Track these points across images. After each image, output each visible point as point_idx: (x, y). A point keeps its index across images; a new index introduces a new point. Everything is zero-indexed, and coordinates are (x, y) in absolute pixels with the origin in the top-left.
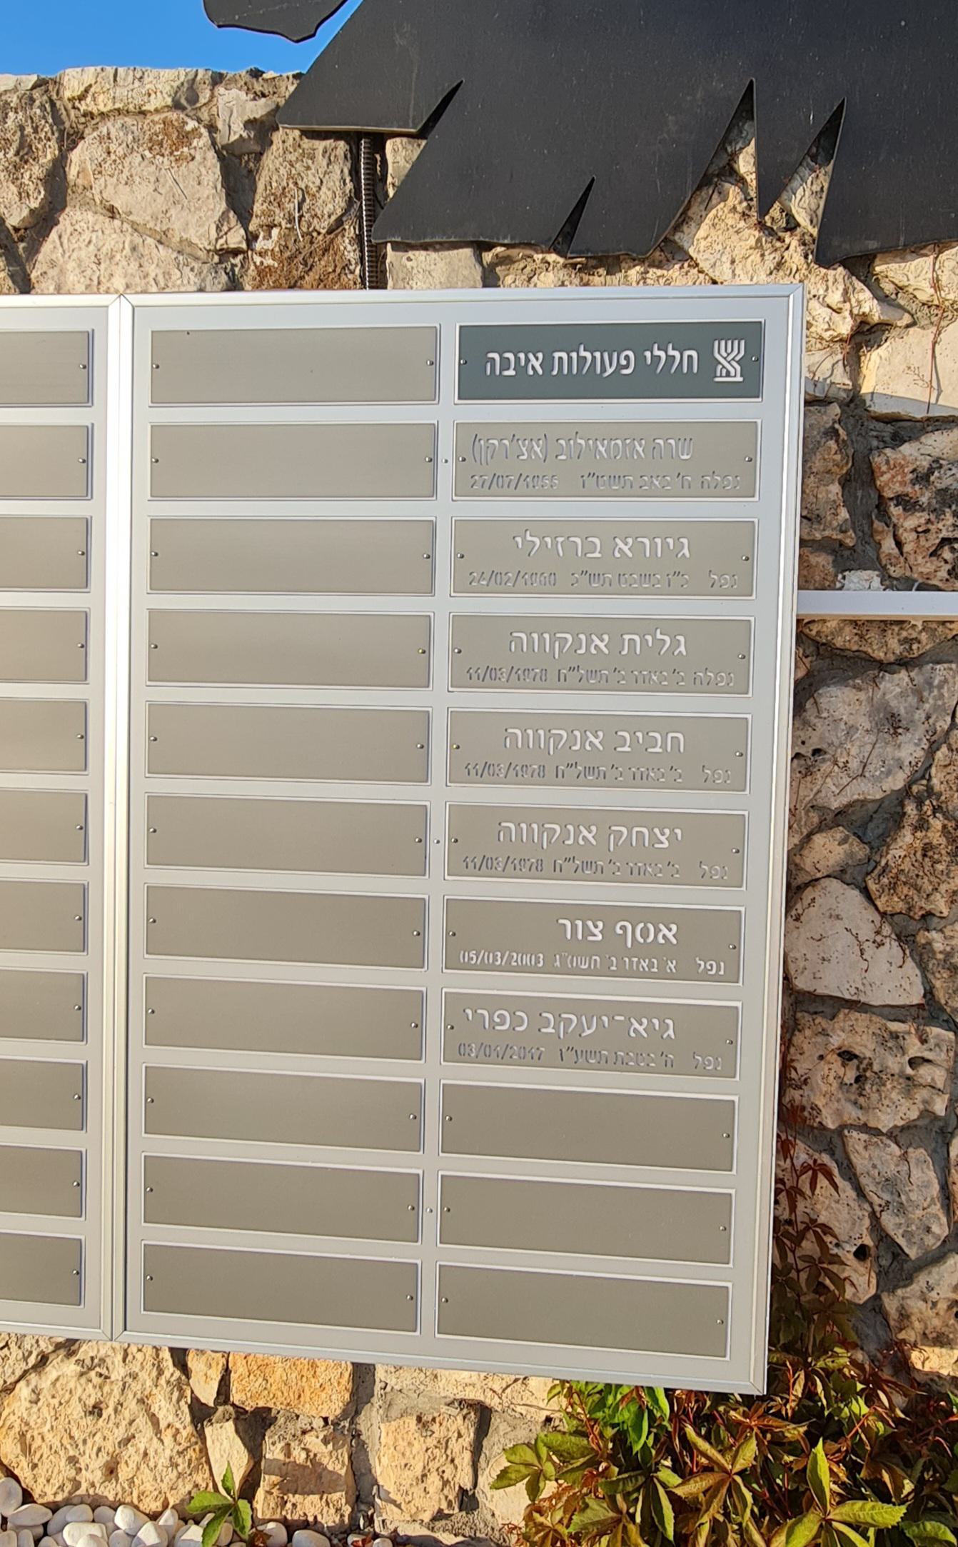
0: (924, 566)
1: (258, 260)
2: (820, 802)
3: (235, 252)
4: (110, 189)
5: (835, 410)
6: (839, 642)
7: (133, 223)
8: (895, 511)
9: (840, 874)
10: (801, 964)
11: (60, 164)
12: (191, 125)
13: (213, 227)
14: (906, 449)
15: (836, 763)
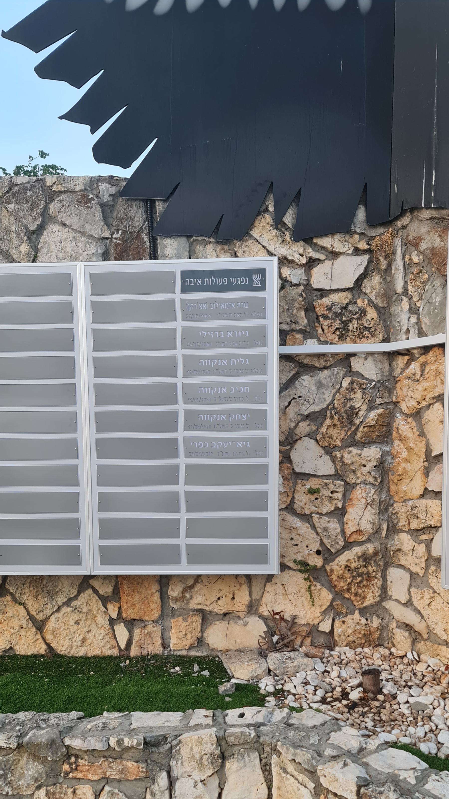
0: (331, 337)
1: (115, 241)
2: (301, 413)
3: (107, 238)
4: (64, 218)
5: (302, 288)
6: (305, 362)
7: (72, 229)
8: (321, 319)
9: (309, 435)
10: (297, 464)
11: (46, 208)
12: (91, 196)
13: (100, 231)
14: (325, 300)
15: (305, 400)
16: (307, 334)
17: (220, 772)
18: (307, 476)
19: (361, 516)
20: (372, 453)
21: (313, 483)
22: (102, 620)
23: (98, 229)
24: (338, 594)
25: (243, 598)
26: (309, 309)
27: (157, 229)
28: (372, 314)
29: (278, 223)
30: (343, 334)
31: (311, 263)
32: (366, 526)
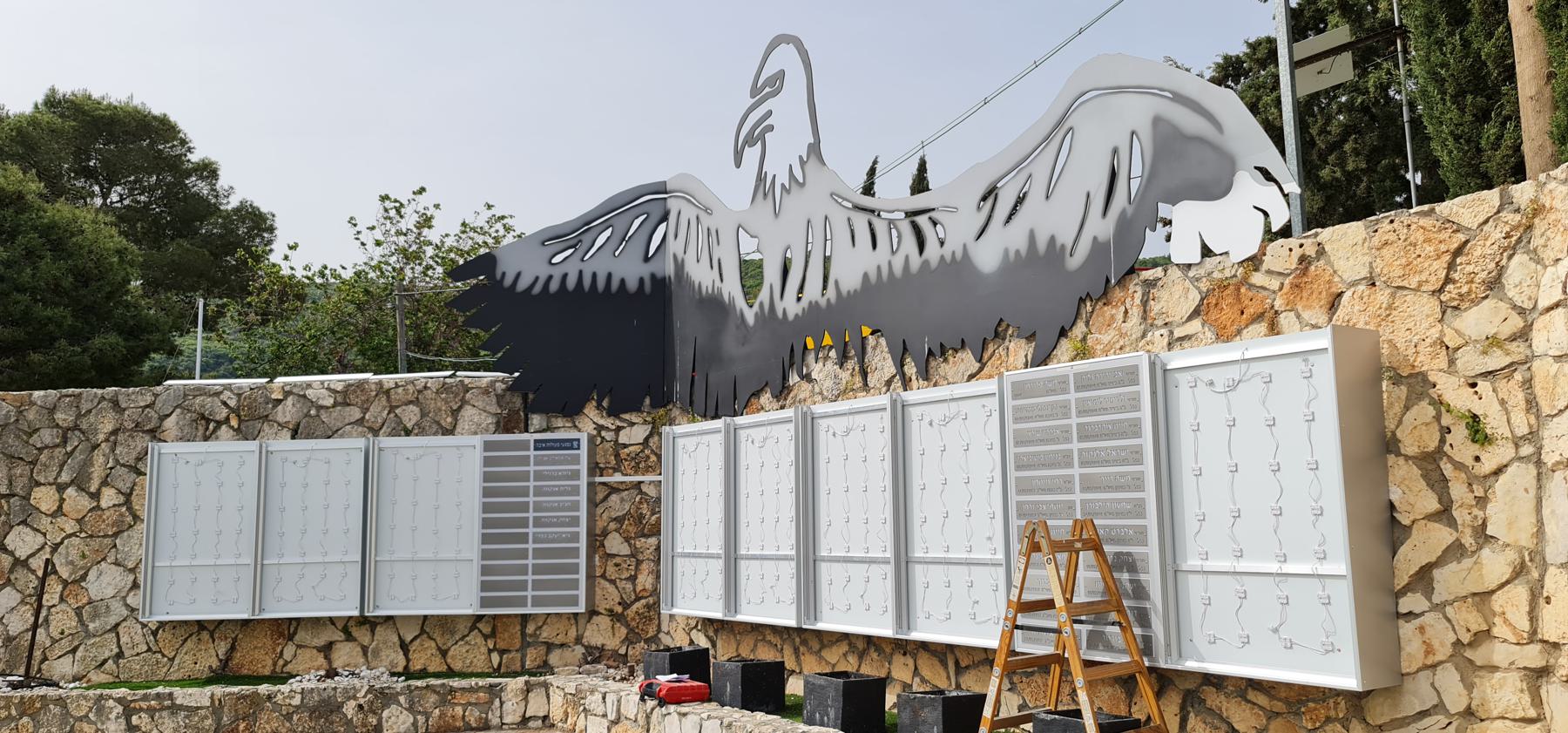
16: (616, 470)
17: (526, 699)
18: (614, 556)
19: (644, 580)
20: (653, 541)
21: (617, 560)
22: (484, 650)
23: (494, 409)
24: (631, 630)
25: (573, 633)
26: (617, 455)
27: (529, 409)
28: (653, 458)
29: (599, 407)
30: (636, 470)
31: (619, 429)
32: (649, 586)
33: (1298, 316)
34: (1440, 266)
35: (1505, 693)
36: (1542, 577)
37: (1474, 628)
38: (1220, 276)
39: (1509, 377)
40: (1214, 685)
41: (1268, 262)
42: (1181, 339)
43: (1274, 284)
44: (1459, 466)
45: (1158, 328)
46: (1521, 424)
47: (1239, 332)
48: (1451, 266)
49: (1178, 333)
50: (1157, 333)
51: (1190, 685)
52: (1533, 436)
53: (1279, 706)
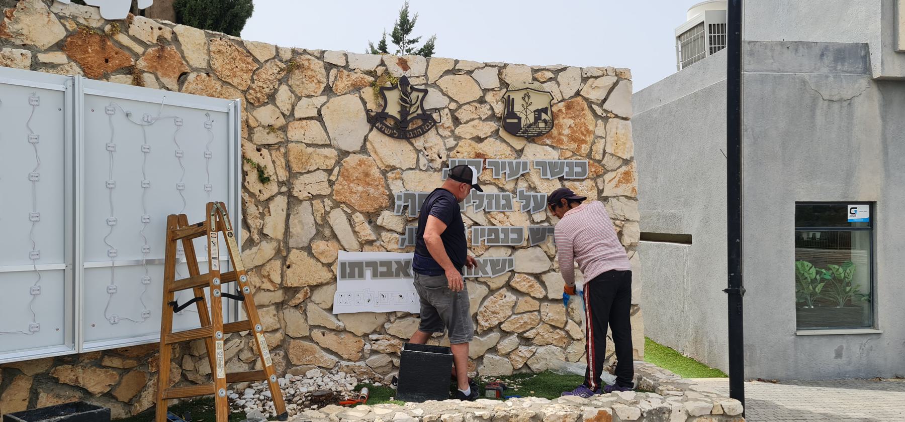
33: (157, 79)
34: (247, 77)
35: (267, 318)
36: (288, 254)
37: (258, 285)
38: (85, 23)
39: (278, 149)
40: (68, 363)
41: (133, 30)
42: (45, 64)
43: (139, 49)
44: (252, 195)
45: (18, 47)
46: (283, 175)
47: (106, 77)
48: (253, 81)
49: (42, 58)
50: (17, 52)
51: (30, 372)
52: (288, 183)
53: (130, 363)
